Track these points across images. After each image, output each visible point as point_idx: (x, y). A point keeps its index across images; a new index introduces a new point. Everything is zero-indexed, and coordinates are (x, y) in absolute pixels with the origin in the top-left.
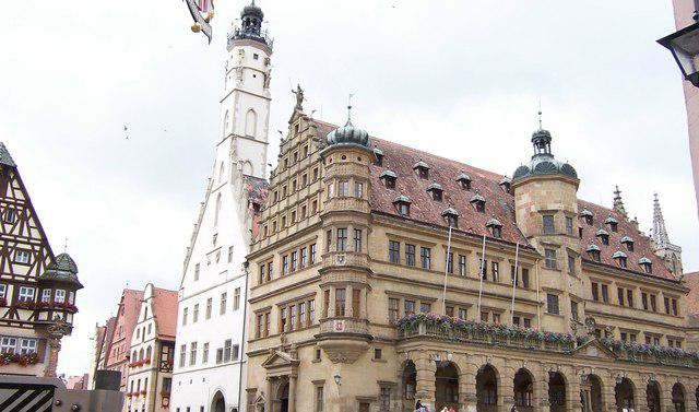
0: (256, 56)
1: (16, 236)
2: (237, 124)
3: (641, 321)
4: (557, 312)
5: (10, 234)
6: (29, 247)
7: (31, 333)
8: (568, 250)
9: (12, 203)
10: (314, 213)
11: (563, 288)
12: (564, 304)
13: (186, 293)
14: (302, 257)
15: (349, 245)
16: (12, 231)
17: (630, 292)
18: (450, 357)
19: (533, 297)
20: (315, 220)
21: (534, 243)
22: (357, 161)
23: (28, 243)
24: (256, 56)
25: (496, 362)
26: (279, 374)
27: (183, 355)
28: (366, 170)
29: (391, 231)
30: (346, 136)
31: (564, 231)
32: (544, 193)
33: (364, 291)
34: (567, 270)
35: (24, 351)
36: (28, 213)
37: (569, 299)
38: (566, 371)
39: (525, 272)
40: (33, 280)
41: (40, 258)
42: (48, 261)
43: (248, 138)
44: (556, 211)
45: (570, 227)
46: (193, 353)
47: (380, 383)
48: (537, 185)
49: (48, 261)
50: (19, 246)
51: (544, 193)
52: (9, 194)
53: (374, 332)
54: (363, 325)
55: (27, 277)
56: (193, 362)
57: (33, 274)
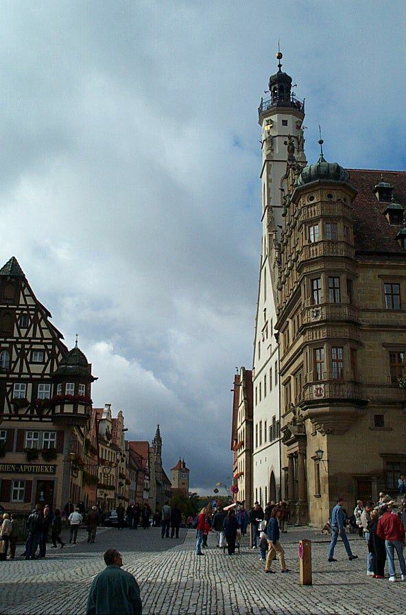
1: (30, 339)
2: (271, 195)
5: (25, 338)
6: (42, 347)
7: (50, 426)
9: (24, 309)
15: (320, 297)
16: (27, 334)
24: (285, 123)
35: (46, 443)
36: (40, 316)
40: (48, 377)
41: (53, 356)
42: (60, 358)
47: (384, 456)
49: (60, 358)
50: (34, 347)
52: (22, 301)
53: (370, 394)
55: (43, 374)
57: (48, 371)
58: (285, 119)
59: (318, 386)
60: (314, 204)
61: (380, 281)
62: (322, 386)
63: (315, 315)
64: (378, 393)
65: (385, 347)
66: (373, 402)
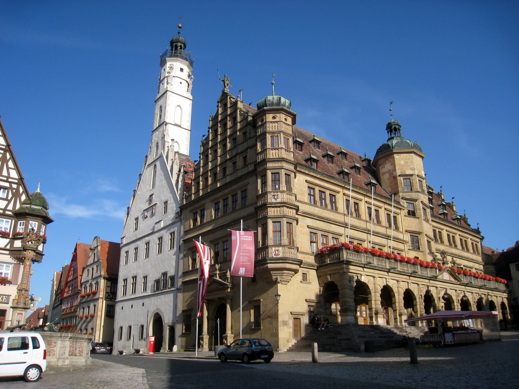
0: (182, 70)
4: (419, 248)
6: (7, 185)
7: (8, 258)
8: (422, 202)
10: (245, 165)
12: (424, 241)
13: (125, 242)
14: (235, 201)
17: (453, 237)
19: (400, 236)
20: (245, 171)
22: (284, 121)
23: (6, 181)
24: (182, 70)
25: (392, 284)
26: (215, 297)
27: (125, 286)
28: (290, 128)
31: (419, 190)
32: (402, 162)
33: (294, 223)
34: (423, 218)
37: (426, 239)
38: (433, 291)
39: (395, 217)
40: (10, 213)
41: (16, 195)
43: (175, 125)
44: (412, 175)
45: (421, 186)
46: (134, 284)
48: (396, 156)
49: (24, 198)
51: (402, 162)
54: (296, 251)
55: (5, 210)
56: (134, 291)
57: (10, 207)
59: (277, 248)
60: (277, 122)
61: (306, 185)
62: (280, 248)
64: (305, 259)
65: (308, 228)
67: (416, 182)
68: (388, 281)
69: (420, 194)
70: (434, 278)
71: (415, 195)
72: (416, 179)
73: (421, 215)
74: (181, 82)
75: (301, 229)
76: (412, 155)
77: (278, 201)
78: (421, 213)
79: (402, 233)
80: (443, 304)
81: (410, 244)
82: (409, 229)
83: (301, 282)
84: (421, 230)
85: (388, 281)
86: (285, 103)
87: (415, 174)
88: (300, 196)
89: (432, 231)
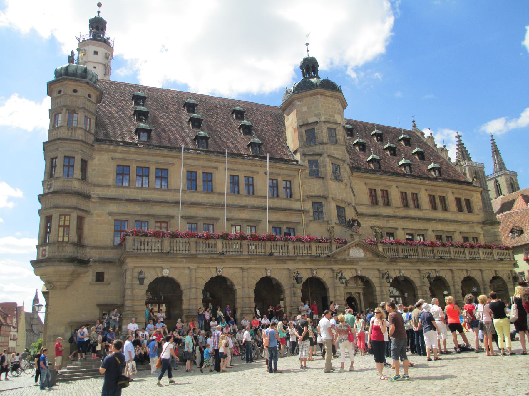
3: (428, 220)
11: (326, 194)
18: (166, 273)
19: (297, 205)
21: (298, 157)
24: (96, 53)
29: (118, 155)
30: (63, 72)
31: (325, 140)
32: (305, 109)
44: (316, 123)
47: (99, 306)
48: (298, 103)
51: (305, 109)
58: (96, 50)
63: (49, 187)
66: (95, 261)
67: (322, 132)
68: (220, 271)
69: (325, 146)
70: (330, 259)
71: (319, 148)
72: (321, 127)
73: (326, 174)
74: (95, 66)
75: (99, 218)
76: (318, 98)
77: (51, 191)
78: (326, 170)
79: (299, 200)
80: (362, 289)
81: (311, 214)
82: (310, 194)
83: (90, 283)
84: (326, 193)
85: (220, 271)
86: (76, 71)
87: (320, 121)
88: (100, 179)
89: (367, 192)
